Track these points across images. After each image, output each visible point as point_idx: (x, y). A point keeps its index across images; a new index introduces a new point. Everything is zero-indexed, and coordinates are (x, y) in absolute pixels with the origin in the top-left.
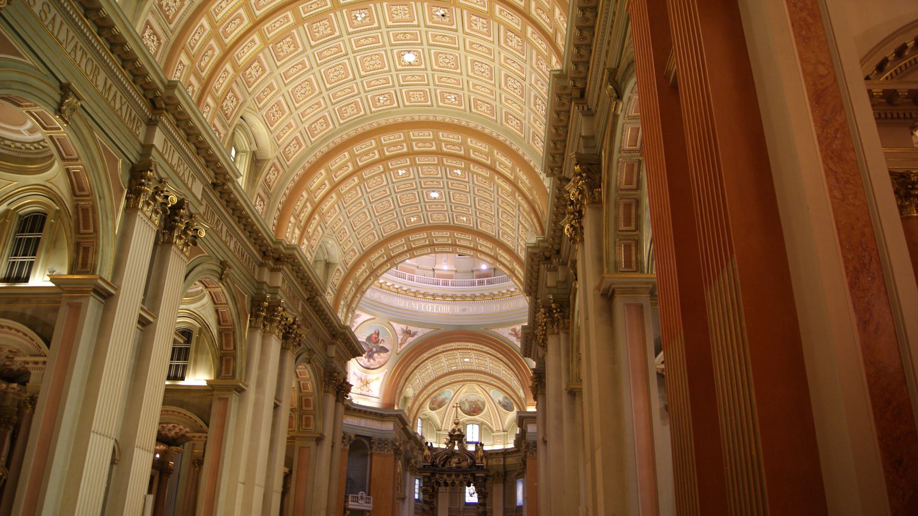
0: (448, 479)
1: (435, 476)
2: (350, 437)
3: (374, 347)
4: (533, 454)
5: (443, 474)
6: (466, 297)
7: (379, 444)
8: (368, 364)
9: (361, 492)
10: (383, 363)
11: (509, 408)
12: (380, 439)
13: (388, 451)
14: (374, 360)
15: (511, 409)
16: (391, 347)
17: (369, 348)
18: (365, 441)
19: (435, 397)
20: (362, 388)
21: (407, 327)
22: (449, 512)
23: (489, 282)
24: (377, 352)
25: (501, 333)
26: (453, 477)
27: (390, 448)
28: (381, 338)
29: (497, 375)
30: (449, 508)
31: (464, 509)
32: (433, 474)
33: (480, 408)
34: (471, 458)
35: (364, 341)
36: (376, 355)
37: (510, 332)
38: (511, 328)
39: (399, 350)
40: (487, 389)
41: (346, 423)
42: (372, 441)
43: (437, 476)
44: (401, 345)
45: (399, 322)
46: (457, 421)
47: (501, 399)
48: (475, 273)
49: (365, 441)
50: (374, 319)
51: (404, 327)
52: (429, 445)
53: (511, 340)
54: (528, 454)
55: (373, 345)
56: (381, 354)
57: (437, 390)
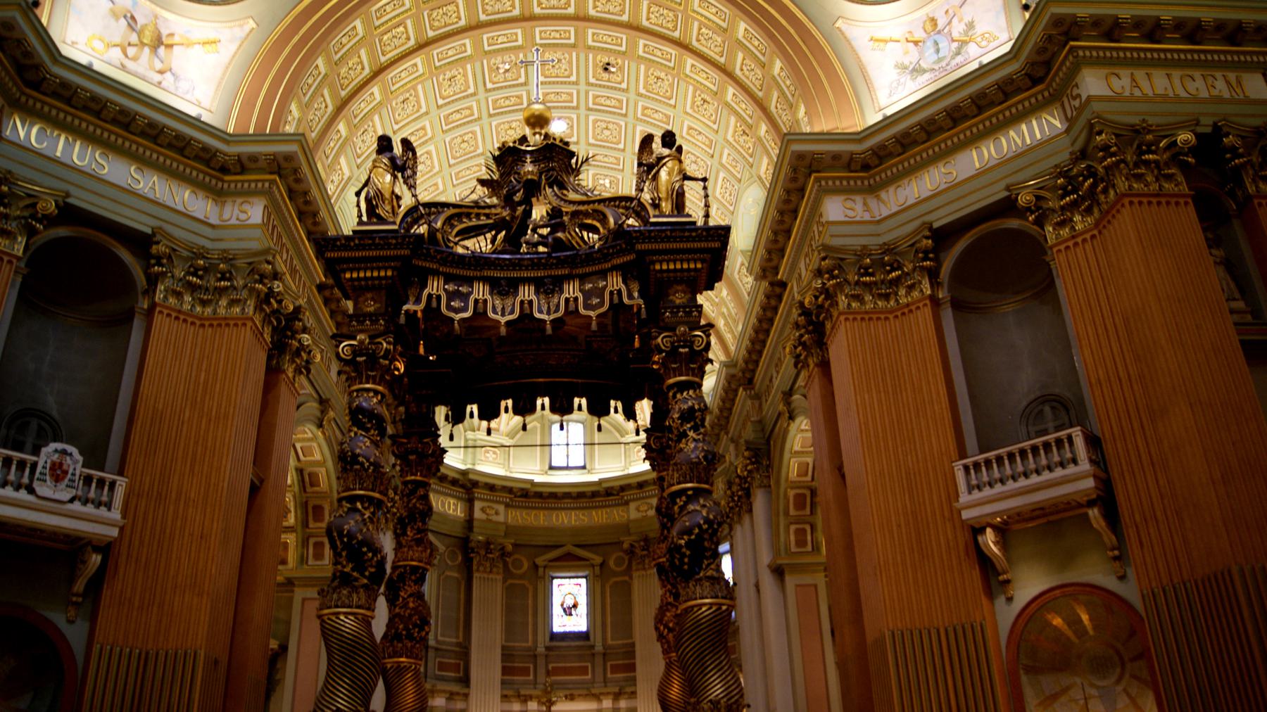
2: (34, 205)
5: (469, 281)
9: (53, 446)
13: (233, 303)
18: (125, 255)
20: (131, 51)
22: (502, 661)
26: (527, 293)
27: (245, 294)
30: (503, 648)
31: (548, 648)
42: (160, 248)
43: (435, 287)
49: (125, 255)
52: (398, 149)
54: (842, 301)
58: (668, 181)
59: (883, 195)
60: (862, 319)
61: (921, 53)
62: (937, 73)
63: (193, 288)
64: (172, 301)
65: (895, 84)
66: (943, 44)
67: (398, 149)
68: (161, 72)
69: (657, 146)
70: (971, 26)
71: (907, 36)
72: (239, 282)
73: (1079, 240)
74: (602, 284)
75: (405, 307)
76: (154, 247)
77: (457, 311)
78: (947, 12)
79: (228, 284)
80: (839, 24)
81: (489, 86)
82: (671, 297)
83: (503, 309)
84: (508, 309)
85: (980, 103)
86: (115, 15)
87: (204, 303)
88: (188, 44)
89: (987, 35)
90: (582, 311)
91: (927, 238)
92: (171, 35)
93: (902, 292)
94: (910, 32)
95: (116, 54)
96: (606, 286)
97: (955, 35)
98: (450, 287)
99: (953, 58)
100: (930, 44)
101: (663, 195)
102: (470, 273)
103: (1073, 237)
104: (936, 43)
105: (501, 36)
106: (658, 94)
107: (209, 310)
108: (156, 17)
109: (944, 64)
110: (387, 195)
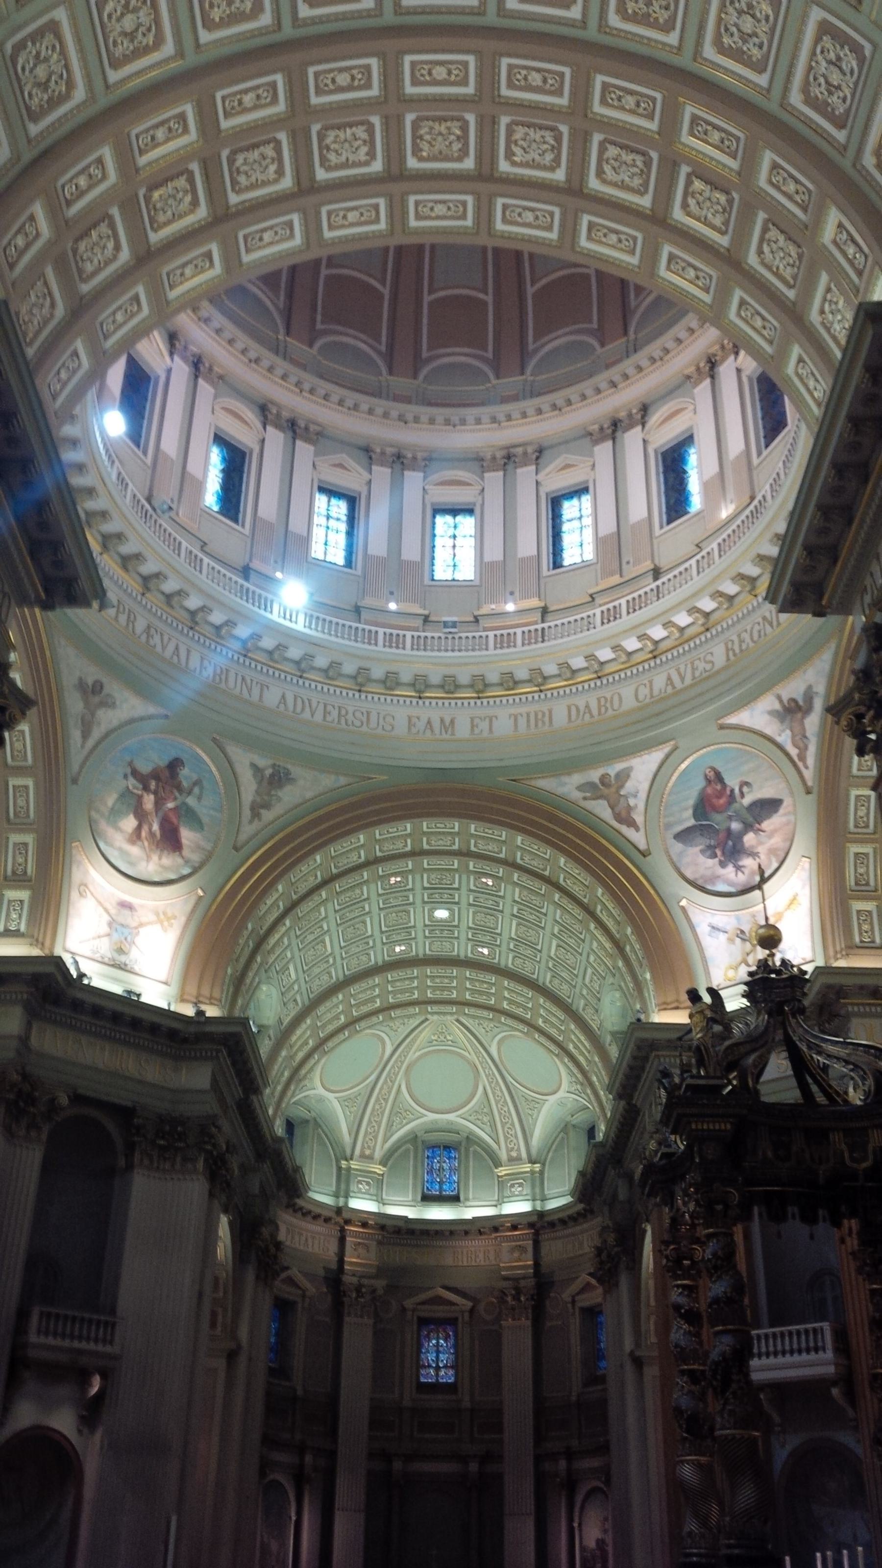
3: (730, 818)
8: (742, 879)
10: (788, 844)
14: (754, 855)
16: (783, 785)
17: (717, 831)
21: (779, 698)
24: (748, 827)
28: (732, 782)
35: (692, 822)
36: (749, 839)
39: (808, 774)
44: (802, 757)
51: (768, 703)
55: (725, 815)
56: (766, 825)
86: (731, 941)
108: (754, 916)
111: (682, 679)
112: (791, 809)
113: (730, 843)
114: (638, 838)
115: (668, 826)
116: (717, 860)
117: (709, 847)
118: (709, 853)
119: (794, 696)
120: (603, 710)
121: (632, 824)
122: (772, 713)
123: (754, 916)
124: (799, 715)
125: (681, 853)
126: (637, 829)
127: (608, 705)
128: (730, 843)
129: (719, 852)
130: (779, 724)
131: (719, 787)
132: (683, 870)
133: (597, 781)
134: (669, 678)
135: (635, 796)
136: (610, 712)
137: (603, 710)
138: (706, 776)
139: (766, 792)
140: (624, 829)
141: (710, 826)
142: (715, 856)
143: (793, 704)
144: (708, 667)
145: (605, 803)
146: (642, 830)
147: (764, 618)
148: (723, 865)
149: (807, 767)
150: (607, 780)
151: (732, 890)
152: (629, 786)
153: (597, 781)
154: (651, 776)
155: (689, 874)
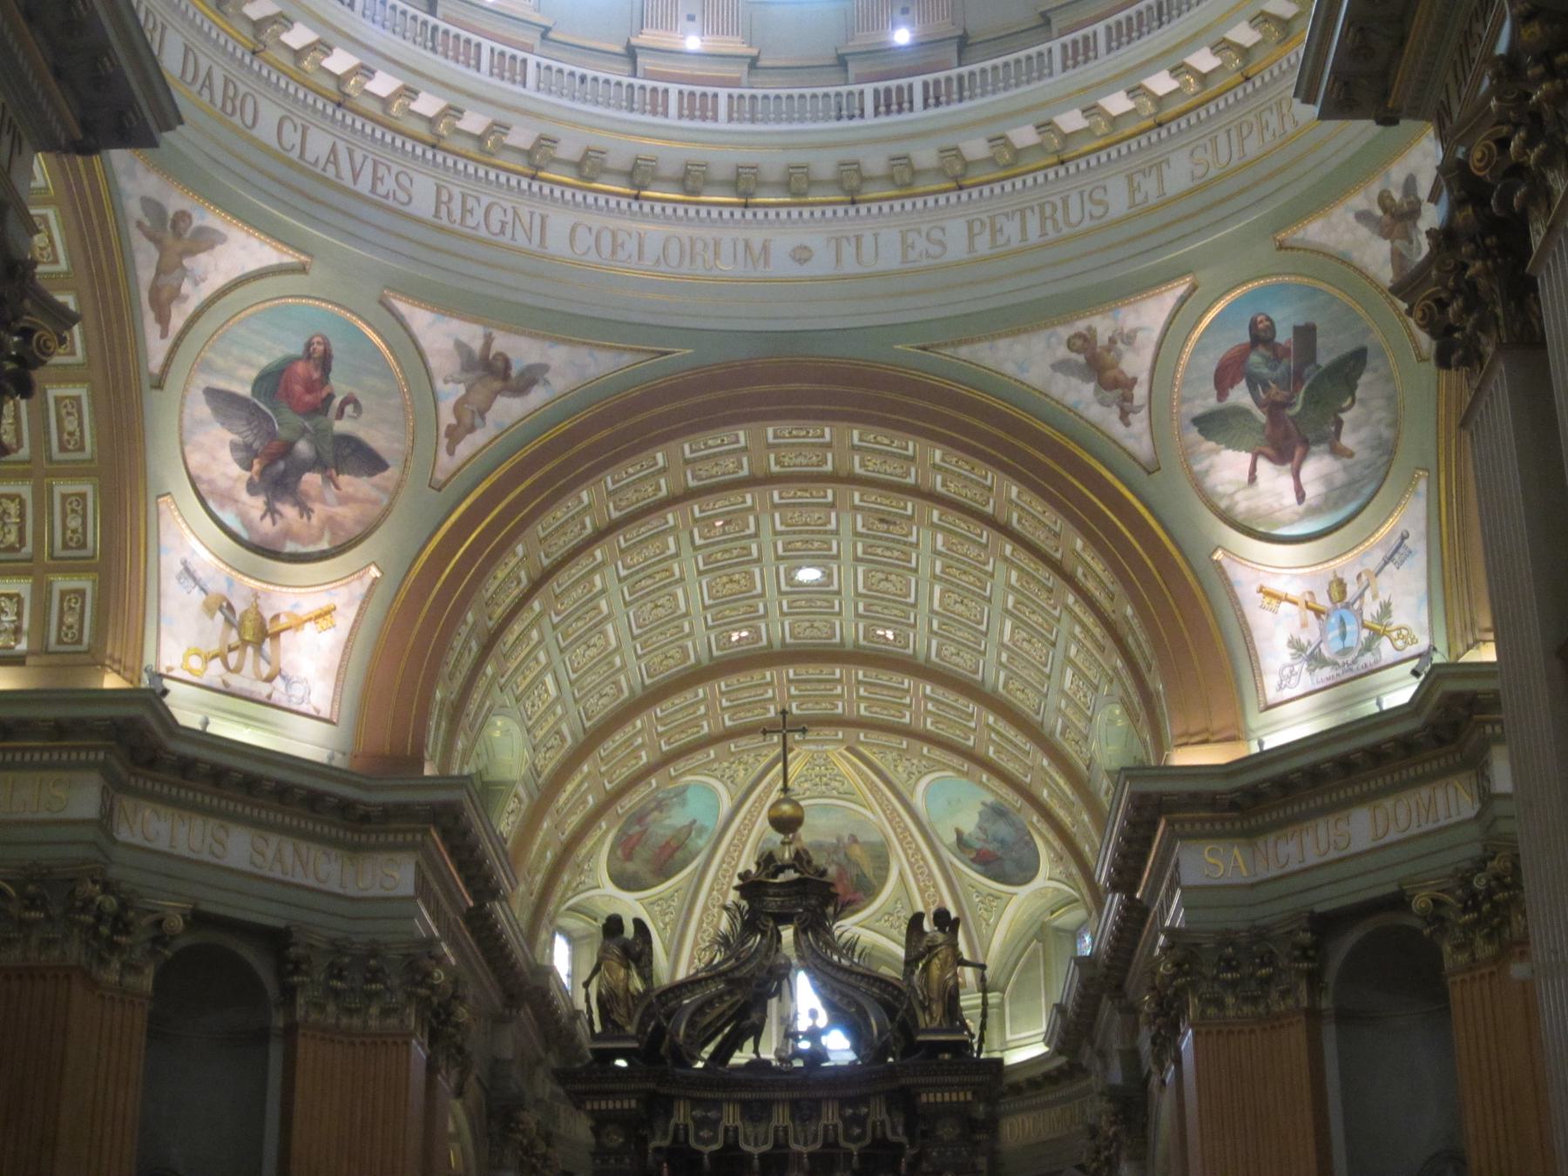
0: (746, 1129)
1: (669, 1114)
2: (159, 923)
3: (303, 432)
4: (1219, 1003)
5: (717, 1104)
6: (813, 183)
7: (336, 972)
10: (358, 530)
11: (1009, 867)
12: (337, 947)
13: (386, 1013)
14: (305, 510)
15: (1023, 872)
17: (272, 435)
19: (639, 817)
20: (233, 658)
21: (488, 340)
23: (934, 97)
24: (318, 464)
25: (1009, 368)
26: (781, 1117)
28: (340, 386)
29: (961, 663)
32: (657, 1106)
33: (862, 877)
34: (890, 1010)
35: (245, 391)
36: (312, 480)
37: (1062, 352)
38: (1065, 332)
39: (446, 463)
40: (899, 776)
41: (138, 840)
43: (682, 1114)
45: (445, 303)
46: (786, 808)
47: (969, 822)
48: (853, 69)
50: (302, 269)
51: (473, 335)
52: (629, 931)
53: (1070, 399)
54: (1193, 1002)
56: (344, 479)
57: (650, 770)
58: (941, 976)
59: (1260, 842)
60: (1219, 1032)
61: (1323, 632)
62: (1340, 671)
63: (336, 993)
64: (314, 1016)
65: (1287, 671)
66: (1351, 627)
67: (629, 931)
68: (269, 679)
69: (927, 925)
70: (1386, 609)
71: (1307, 598)
72: (395, 981)
73: (1477, 974)
74: (864, 1110)
75: (653, 1144)
76: (291, 950)
77: (707, 1142)
78: (1359, 576)
79: (380, 986)
80: (1219, 555)
81: (698, 542)
82: (940, 1133)
83: (756, 1139)
84: (761, 1138)
85: (1376, 756)
87: (350, 1012)
88: (297, 625)
89: (1404, 632)
90: (842, 1142)
91: (1305, 930)
92: (276, 617)
93: (1274, 995)
94: (1311, 593)
95: (216, 665)
96: (868, 1114)
97: (1367, 617)
98: (698, 1113)
99: (1361, 653)
100: (1333, 620)
101: (934, 995)
102: (718, 1095)
103: (1470, 969)
104: (1342, 623)
105: (720, 504)
106: (966, 555)
107: (356, 1022)
109: (1350, 659)
110: (621, 993)
111: (356, 177)
112: (391, 485)
113: (281, 465)
114: (156, 348)
115: (208, 367)
116: (247, 475)
117: (248, 447)
118: (241, 455)
119: (511, 356)
120: (229, 109)
121: (163, 319)
122: (460, 346)
123: (256, 596)
124: (497, 385)
125: (201, 422)
126: (164, 335)
127: (238, 103)
128: (281, 465)
129: (256, 467)
130: (458, 368)
131: (316, 375)
132: (187, 449)
133: (171, 213)
134: (333, 150)
135: (196, 283)
136: (236, 119)
137: (229, 109)
138: (309, 345)
139: (377, 438)
140: (149, 317)
141: (269, 419)
142: (249, 468)
143: (500, 364)
144: (402, 197)
145: (156, 256)
146: (168, 342)
147: (516, 213)
148: (252, 488)
149: (451, 452)
150: (182, 225)
151: (244, 534)
152: (200, 262)
153: (171, 213)
154: (235, 274)
155: (195, 460)
